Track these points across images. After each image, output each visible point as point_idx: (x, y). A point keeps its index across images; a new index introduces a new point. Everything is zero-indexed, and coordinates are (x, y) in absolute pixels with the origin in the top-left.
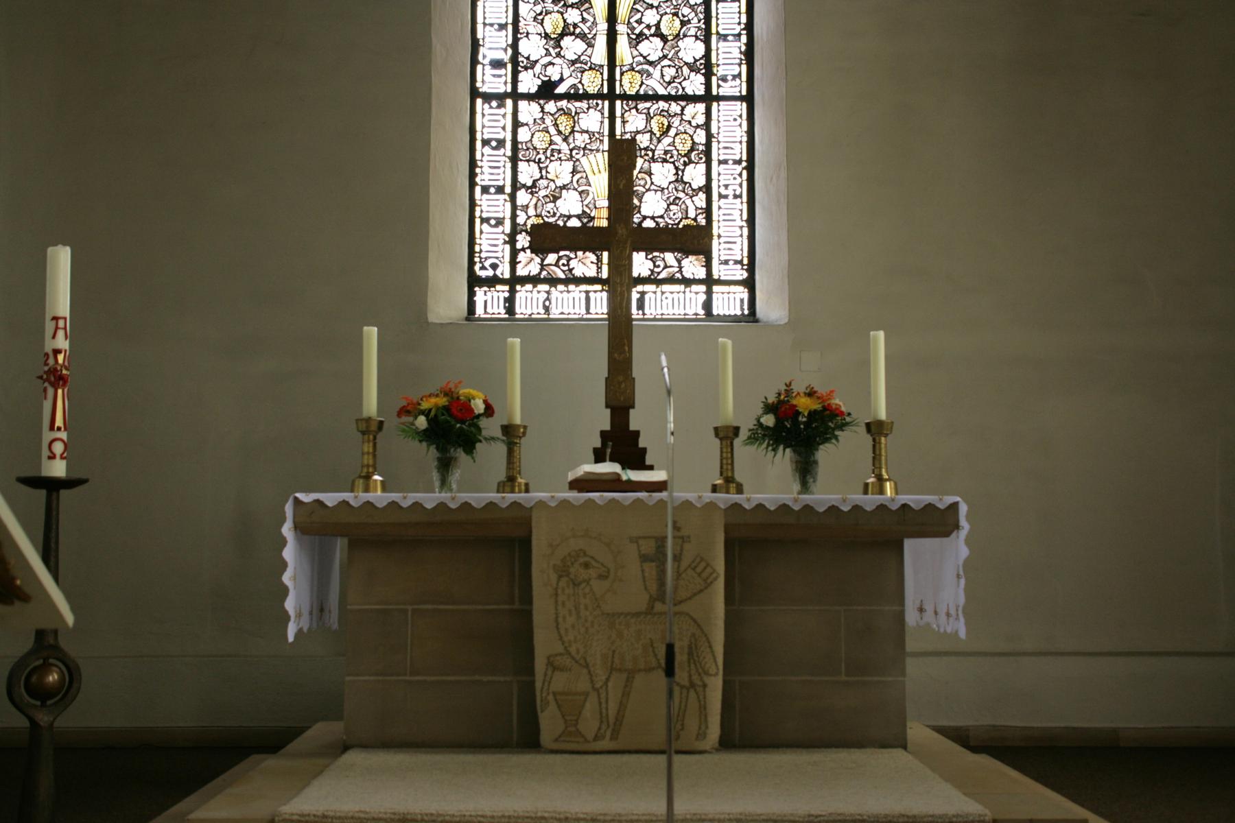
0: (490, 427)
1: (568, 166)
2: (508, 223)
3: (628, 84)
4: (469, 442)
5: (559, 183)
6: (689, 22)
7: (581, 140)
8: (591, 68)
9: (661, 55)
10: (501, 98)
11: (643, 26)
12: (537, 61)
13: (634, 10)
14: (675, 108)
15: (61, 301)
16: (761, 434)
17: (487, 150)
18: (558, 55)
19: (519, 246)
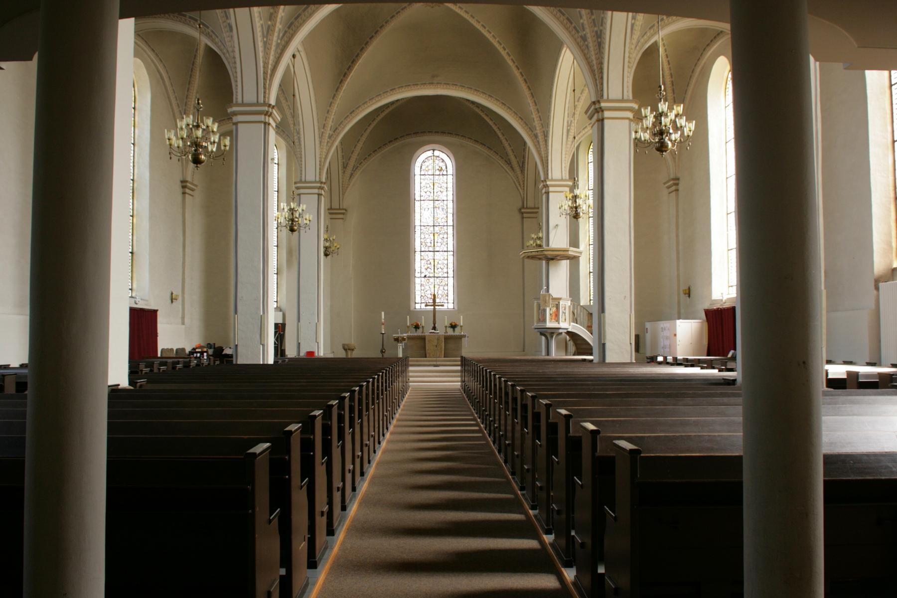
0: (421, 326)
3: (436, 275)
4: (419, 328)
7: (430, 283)
14: (443, 278)
15: (383, 317)
16: (449, 327)
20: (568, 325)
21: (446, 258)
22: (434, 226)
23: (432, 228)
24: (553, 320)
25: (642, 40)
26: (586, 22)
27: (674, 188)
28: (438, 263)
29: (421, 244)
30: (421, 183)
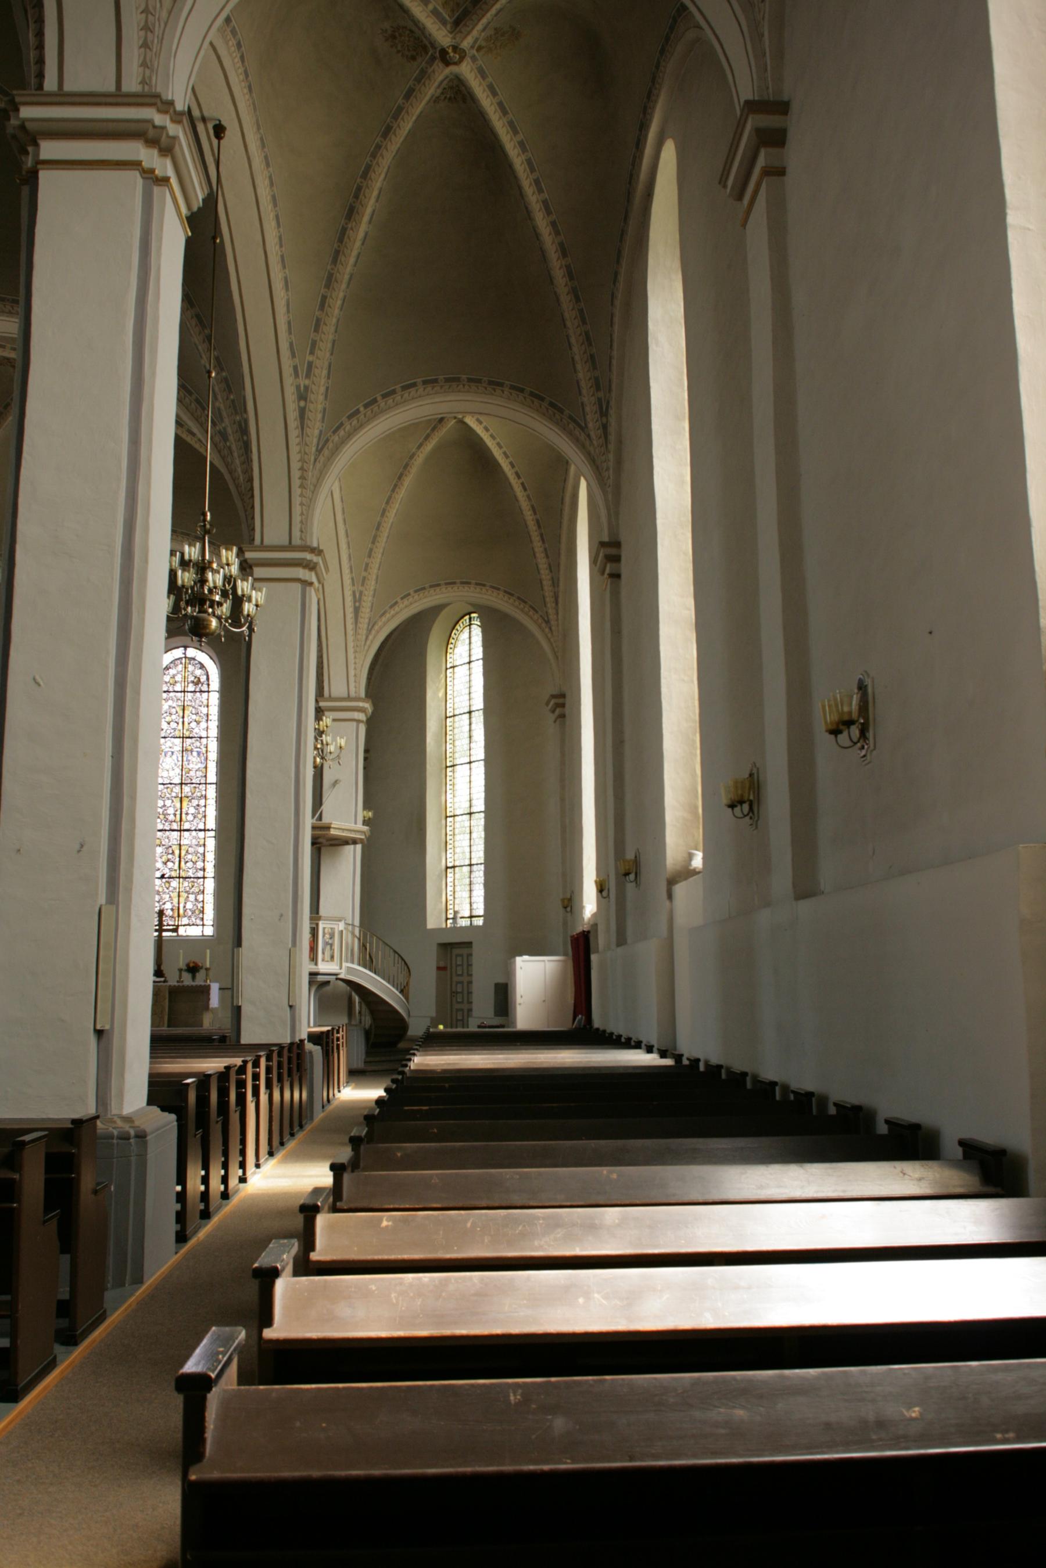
1: (168, 896)
3: (183, 874)
7: (171, 889)
14: (195, 880)
20: (338, 968)
21: (202, 842)
22: (181, 784)
23: (177, 789)
25: (336, 438)
26: (222, 407)
27: (558, 711)
28: (187, 851)
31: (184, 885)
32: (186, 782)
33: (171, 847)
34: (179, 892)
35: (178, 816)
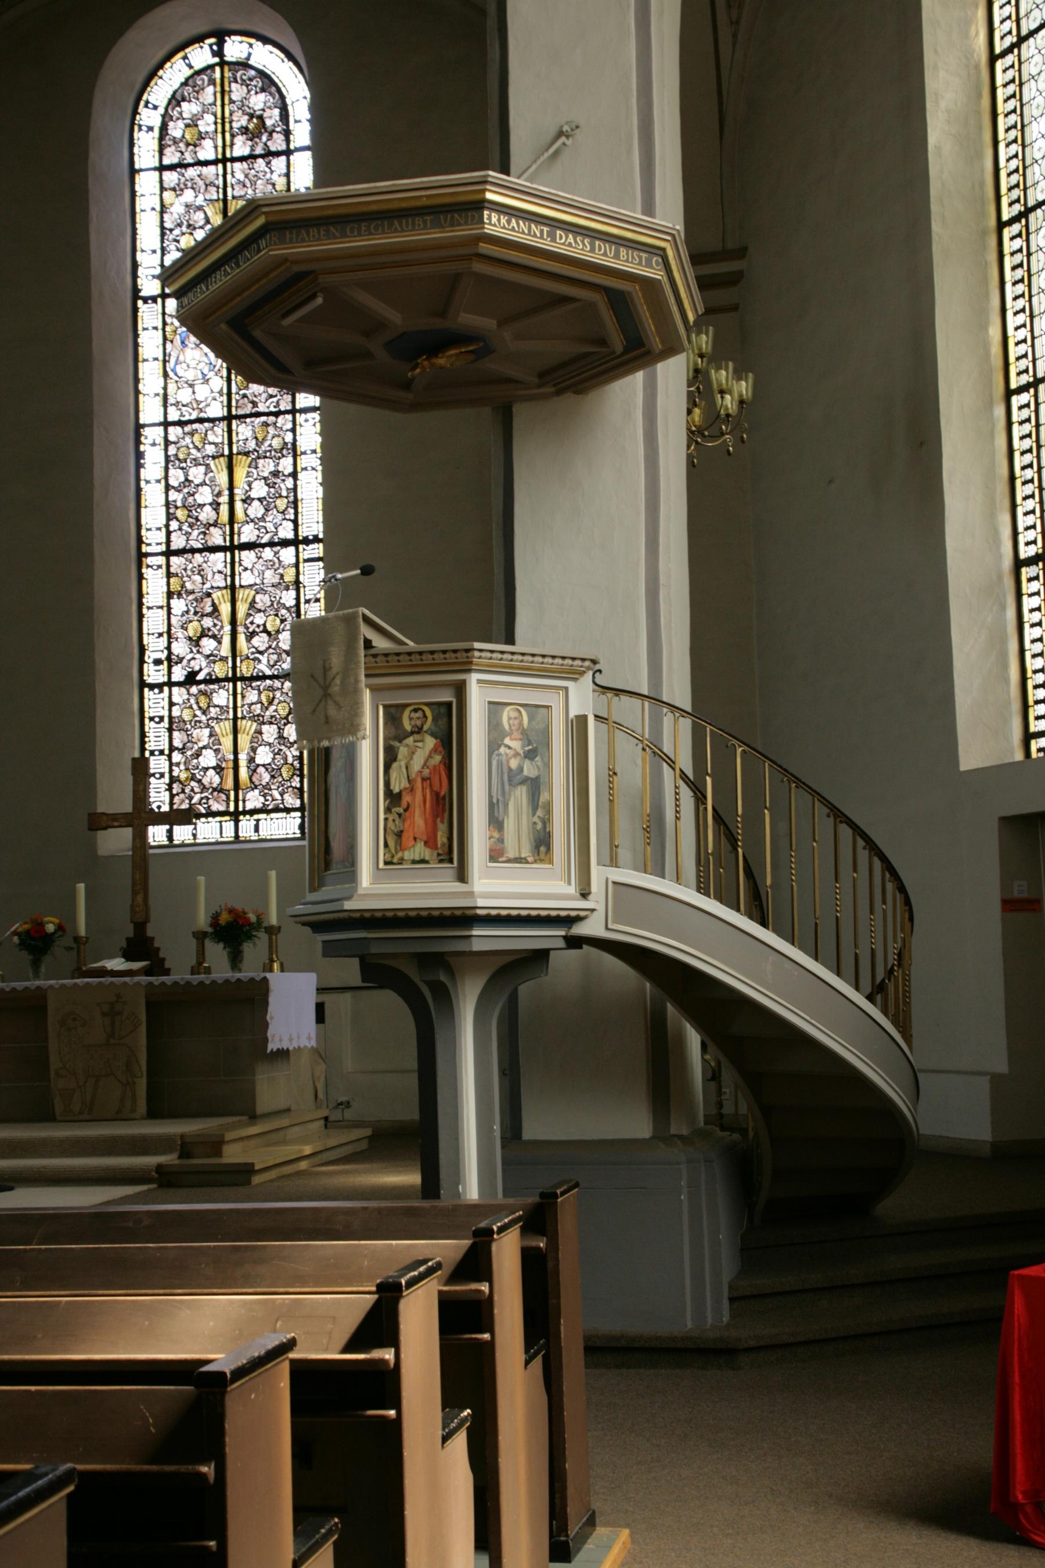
1: (207, 731)
2: (167, 776)
5: (201, 745)
6: (285, 620)
8: (220, 660)
9: (267, 646)
10: (160, 686)
11: (255, 625)
12: (184, 658)
13: (249, 615)
17: (153, 724)
18: (198, 652)
19: (174, 792)
20: (572, 890)
21: (290, 576)
22: (229, 418)
24: (419, 850)
28: (252, 604)
29: (170, 517)
30: (163, 209)
31: (248, 701)
32: (241, 412)
33: (209, 595)
34: (235, 719)
35: (224, 509)
